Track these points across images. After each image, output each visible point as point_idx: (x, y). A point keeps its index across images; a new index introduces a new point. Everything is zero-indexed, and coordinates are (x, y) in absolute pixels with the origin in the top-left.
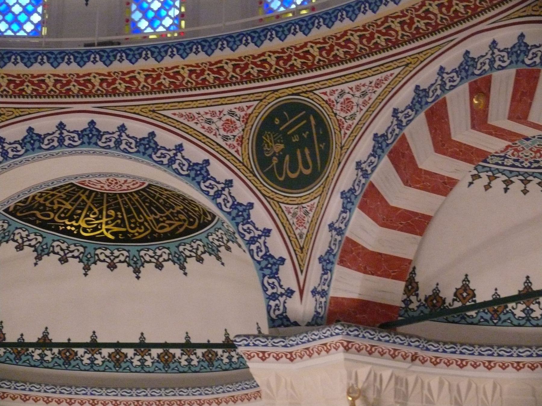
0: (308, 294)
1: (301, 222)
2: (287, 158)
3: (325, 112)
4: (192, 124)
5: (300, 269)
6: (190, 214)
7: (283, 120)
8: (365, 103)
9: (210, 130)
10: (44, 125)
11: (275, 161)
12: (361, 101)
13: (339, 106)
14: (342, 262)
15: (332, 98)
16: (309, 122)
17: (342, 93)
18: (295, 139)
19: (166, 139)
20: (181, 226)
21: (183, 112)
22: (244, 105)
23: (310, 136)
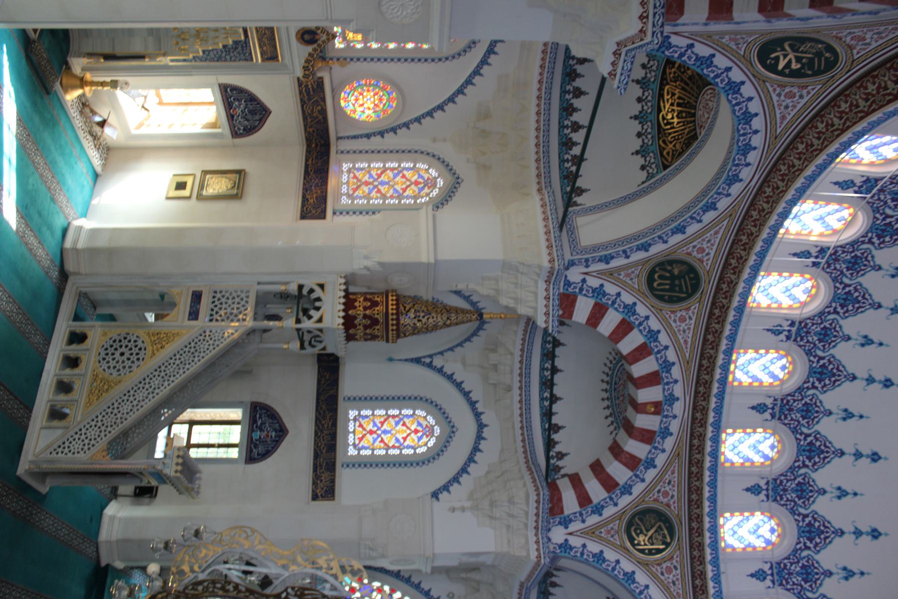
0: (582, 276)
1: (627, 275)
2: (668, 275)
3: (685, 304)
4: (712, 232)
5: (600, 274)
6: (669, 127)
7: (691, 279)
8: (679, 330)
9: (703, 240)
10: (753, 157)
11: (669, 268)
12: (681, 328)
13: (684, 314)
14: (596, 304)
15: (690, 312)
16: (683, 293)
17: (690, 318)
18: (677, 282)
19: (709, 216)
20: (664, 107)
21: (722, 230)
22: (710, 262)
23: (675, 292)
